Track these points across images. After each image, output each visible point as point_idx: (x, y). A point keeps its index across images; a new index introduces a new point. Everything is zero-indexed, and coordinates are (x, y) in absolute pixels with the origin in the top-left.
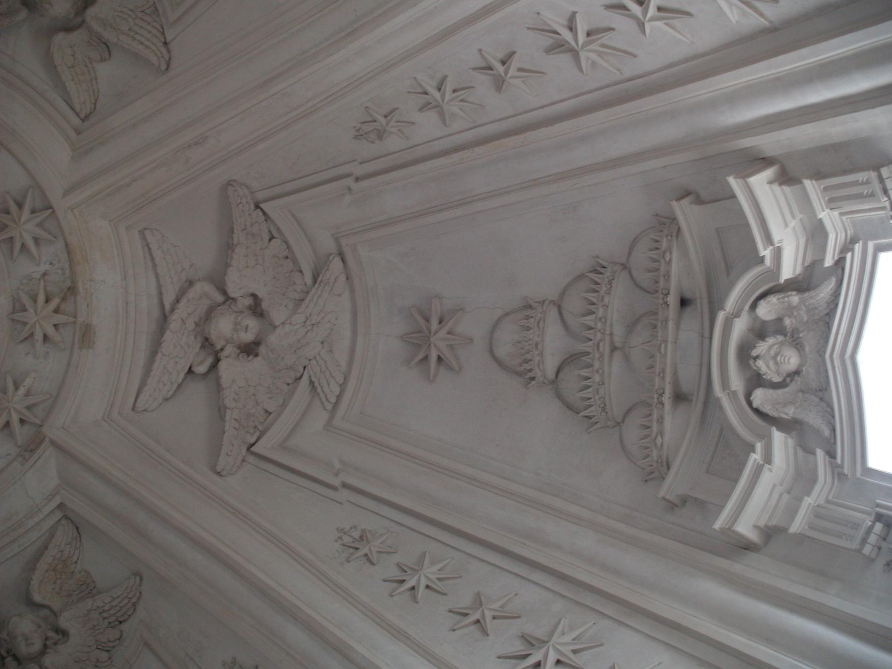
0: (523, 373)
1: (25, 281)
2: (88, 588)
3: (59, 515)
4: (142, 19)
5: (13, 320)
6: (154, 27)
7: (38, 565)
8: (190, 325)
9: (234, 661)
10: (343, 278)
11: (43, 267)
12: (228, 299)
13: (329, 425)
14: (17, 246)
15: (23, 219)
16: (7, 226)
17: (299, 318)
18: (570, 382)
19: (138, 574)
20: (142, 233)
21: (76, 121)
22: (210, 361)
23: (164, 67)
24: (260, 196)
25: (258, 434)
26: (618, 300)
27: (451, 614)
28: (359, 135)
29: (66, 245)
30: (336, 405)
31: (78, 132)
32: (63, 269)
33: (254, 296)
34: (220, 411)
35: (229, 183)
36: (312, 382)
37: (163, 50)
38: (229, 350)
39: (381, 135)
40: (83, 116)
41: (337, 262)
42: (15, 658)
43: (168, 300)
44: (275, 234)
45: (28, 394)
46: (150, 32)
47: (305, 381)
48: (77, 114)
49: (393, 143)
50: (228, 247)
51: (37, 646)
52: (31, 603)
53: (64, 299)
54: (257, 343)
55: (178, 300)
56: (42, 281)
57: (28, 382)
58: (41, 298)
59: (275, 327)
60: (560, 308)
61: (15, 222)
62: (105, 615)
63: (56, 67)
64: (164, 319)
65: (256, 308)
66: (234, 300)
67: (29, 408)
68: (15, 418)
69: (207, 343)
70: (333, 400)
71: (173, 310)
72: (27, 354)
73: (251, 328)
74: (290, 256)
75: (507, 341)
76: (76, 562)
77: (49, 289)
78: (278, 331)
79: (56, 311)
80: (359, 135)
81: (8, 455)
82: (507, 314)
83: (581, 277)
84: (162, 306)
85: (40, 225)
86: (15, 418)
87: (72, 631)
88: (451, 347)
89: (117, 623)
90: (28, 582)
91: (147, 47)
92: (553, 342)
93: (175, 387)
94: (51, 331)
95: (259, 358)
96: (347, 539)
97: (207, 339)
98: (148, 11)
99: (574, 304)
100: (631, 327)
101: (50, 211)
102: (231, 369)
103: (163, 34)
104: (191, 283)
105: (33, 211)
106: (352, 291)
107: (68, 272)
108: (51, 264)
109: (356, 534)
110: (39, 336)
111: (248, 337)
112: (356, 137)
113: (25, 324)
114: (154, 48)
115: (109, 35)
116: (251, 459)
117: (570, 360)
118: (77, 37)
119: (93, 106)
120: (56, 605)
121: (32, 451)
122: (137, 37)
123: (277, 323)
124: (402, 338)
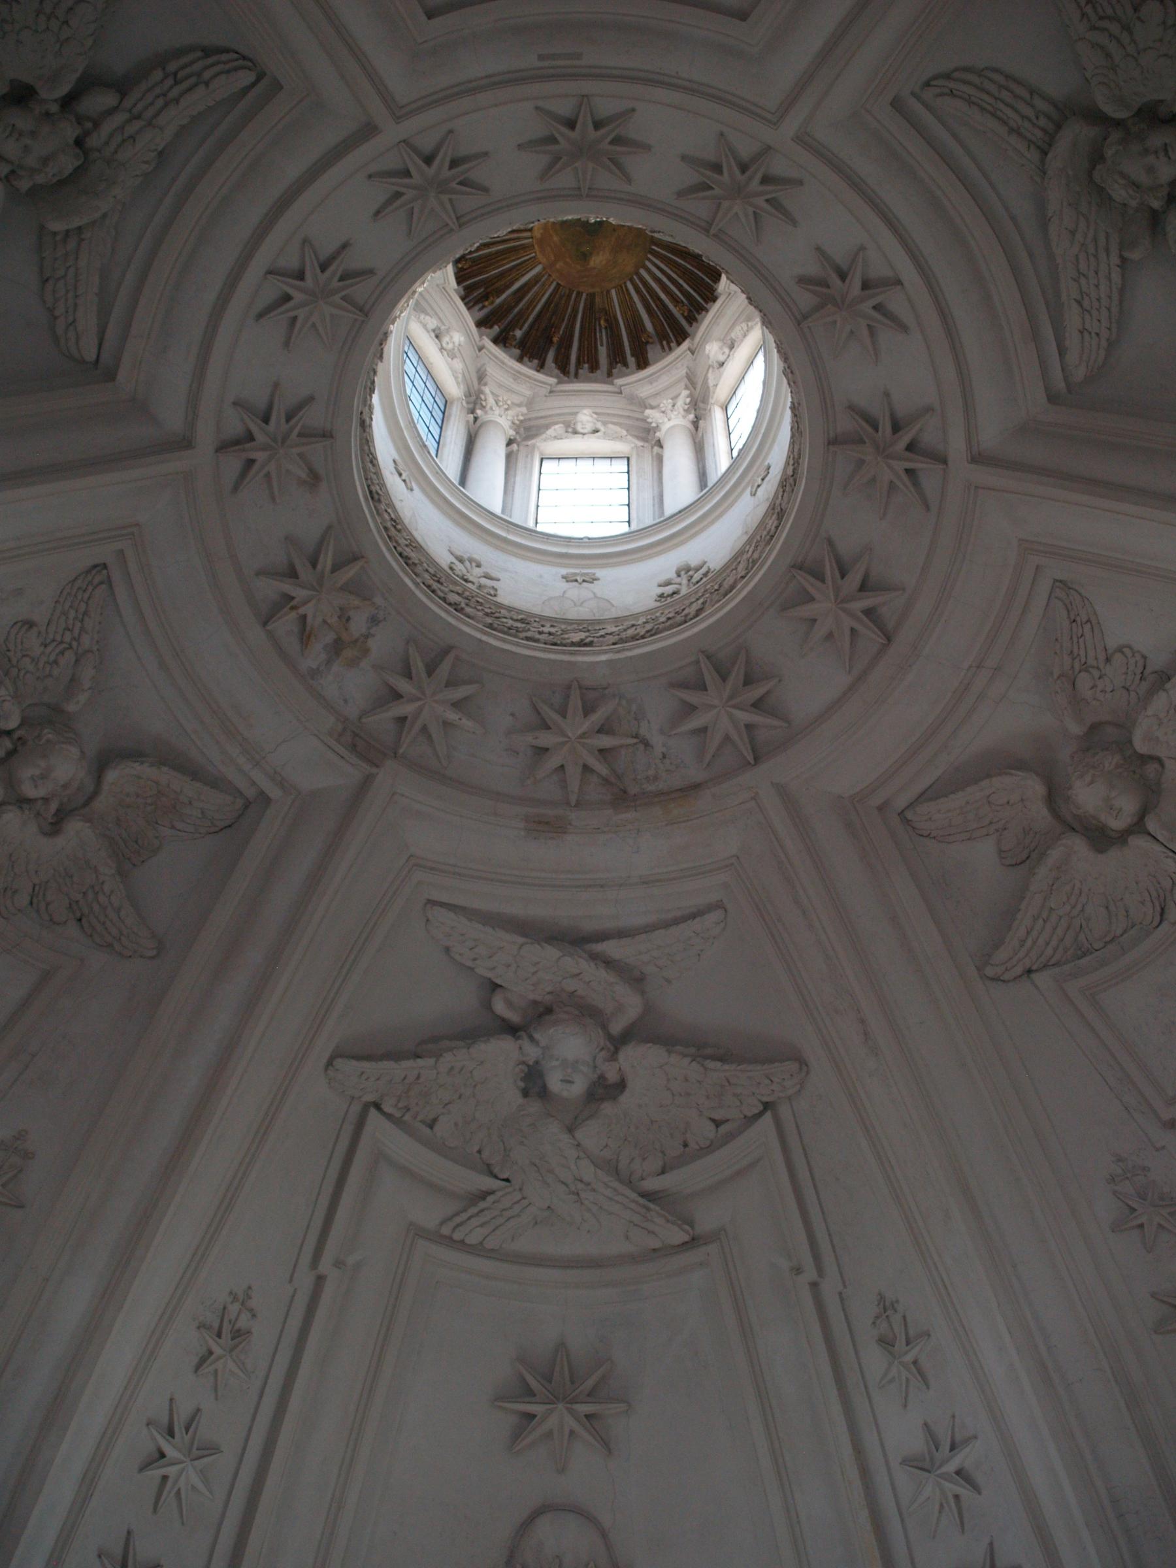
1: (634, 708)
3: (250, 793)
4: (1068, 928)
5: (569, 687)
6: (1055, 950)
7: (165, 769)
8: (571, 985)
9: (28, 1155)
10: (657, 1244)
11: (656, 740)
12: (618, 1042)
13: (418, 1232)
14: (693, 698)
15: (739, 714)
16: (724, 679)
17: (588, 1171)
20: (719, 906)
21: (901, 802)
22: (514, 1017)
23: (990, 971)
24: (784, 1111)
25: (398, 1115)
27: (125, 1533)
28: (886, 1307)
29: (697, 787)
30: (449, 1242)
31: (880, 809)
32: (656, 778)
33: (621, 1085)
34: (428, 1044)
35: (802, 1062)
36: (484, 1195)
37: (1019, 970)
38: (532, 1053)
39: (886, 1342)
40: (909, 815)
41: (678, 1236)
42: (11, 754)
43: (610, 948)
44: (723, 1129)
45: (446, 724)
46: (1048, 944)
47: (488, 1183)
48: (911, 805)
49: (875, 1360)
50: (703, 1047)
51: (29, 791)
52: (101, 764)
53: (606, 781)
54: (544, 1093)
55: (609, 963)
56: (635, 741)
57: (467, 723)
58: (606, 741)
59: (570, 1130)
61: (731, 698)
62: (91, 895)
63: (989, 776)
64: (576, 940)
66: (613, 1057)
67: (424, 729)
68: (406, 709)
69: (542, 1012)
70: (457, 1236)
71: (594, 957)
72: (513, 715)
73: (568, 1086)
74: (688, 1154)
76: (173, 827)
77: (623, 752)
78: (566, 1137)
79: (586, 768)
80: (886, 1307)
81: (346, 701)
82: (604, 1535)
84: (603, 936)
85: (727, 738)
86: (406, 709)
87: (60, 841)
88: (549, 1435)
89: (78, 915)
90: (136, 755)
91: (1023, 942)
93: (469, 964)
94: (553, 762)
95: (520, 1100)
96: (234, 1308)
97: (549, 1010)
98: (1082, 937)
101: (751, 759)
102: (500, 1057)
103: (1045, 966)
104: (637, 980)
105: (749, 727)
106: (634, 1259)
107: (651, 788)
108: (664, 757)
109: (243, 1322)
110: (546, 739)
111: (554, 1083)
112: (881, 1298)
113: (563, 714)
114: (1021, 954)
116: (356, 1108)
118: (1039, 813)
119: (926, 833)
120: (102, 803)
121: (353, 748)
122: (1041, 921)
123: (579, 1134)
124: (561, 1346)
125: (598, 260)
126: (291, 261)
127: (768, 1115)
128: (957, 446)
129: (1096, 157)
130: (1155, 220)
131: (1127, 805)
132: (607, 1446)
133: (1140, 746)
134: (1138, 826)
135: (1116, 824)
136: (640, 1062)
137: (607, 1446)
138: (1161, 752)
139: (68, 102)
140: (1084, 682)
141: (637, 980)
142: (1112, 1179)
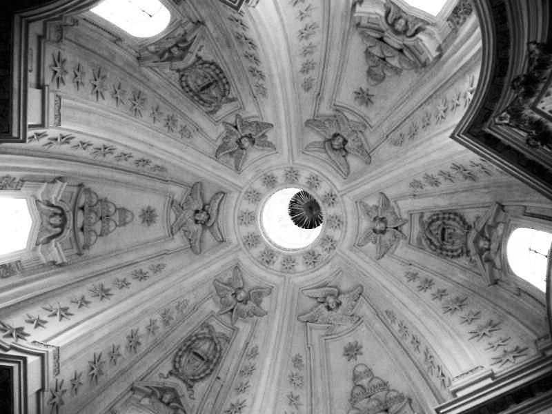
0: (355, 378)
2: (258, 303)
12: (337, 298)
13: (323, 336)
18: (357, 391)
19: (267, 313)
22: (322, 301)
26: (381, 394)
28: (386, 312)
30: (327, 335)
38: (326, 304)
39: (389, 317)
41: (357, 319)
43: (330, 285)
47: (327, 325)
49: (389, 321)
51: (240, 300)
55: (331, 287)
60: (372, 379)
64: (325, 285)
65: (339, 304)
69: (325, 298)
74: (353, 307)
75: (361, 369)
80: (386, 312)
83: (382, 380)
92: (365, 382)
99: (375, 382)
100: (375, 399)
104: (336, 287)
111: (331, 305)
115: (378, 242)
117: (361, 386)
125: (314, 213)
126: (240, 215)
127: (361, 296)
128: (337, 193)
129: (332, 145)
130: (344, 149)
131: (383, 225)
132: (361, 354)
133: (381, 217)
134: (386, 228)
135: (383, 229)
136: (342, 298)
137: (361, 354)
138: (384, 216)
139: (203, 209)
140: (370, 213)
141: (336, 287)
142: (406, 276)
